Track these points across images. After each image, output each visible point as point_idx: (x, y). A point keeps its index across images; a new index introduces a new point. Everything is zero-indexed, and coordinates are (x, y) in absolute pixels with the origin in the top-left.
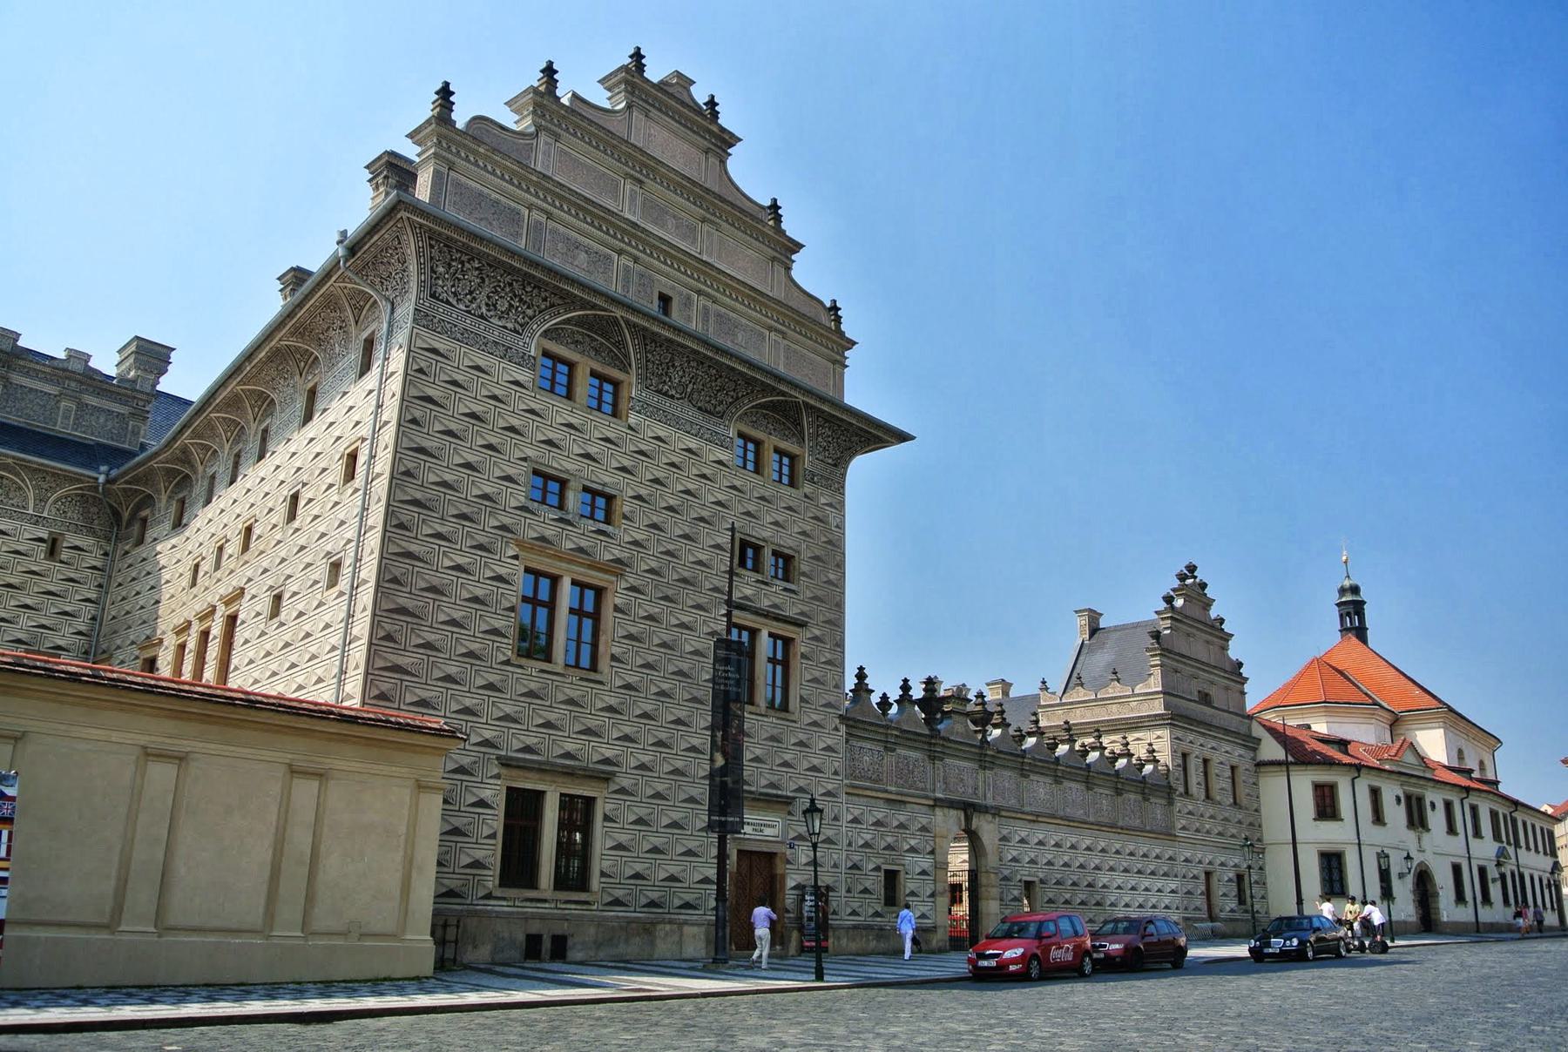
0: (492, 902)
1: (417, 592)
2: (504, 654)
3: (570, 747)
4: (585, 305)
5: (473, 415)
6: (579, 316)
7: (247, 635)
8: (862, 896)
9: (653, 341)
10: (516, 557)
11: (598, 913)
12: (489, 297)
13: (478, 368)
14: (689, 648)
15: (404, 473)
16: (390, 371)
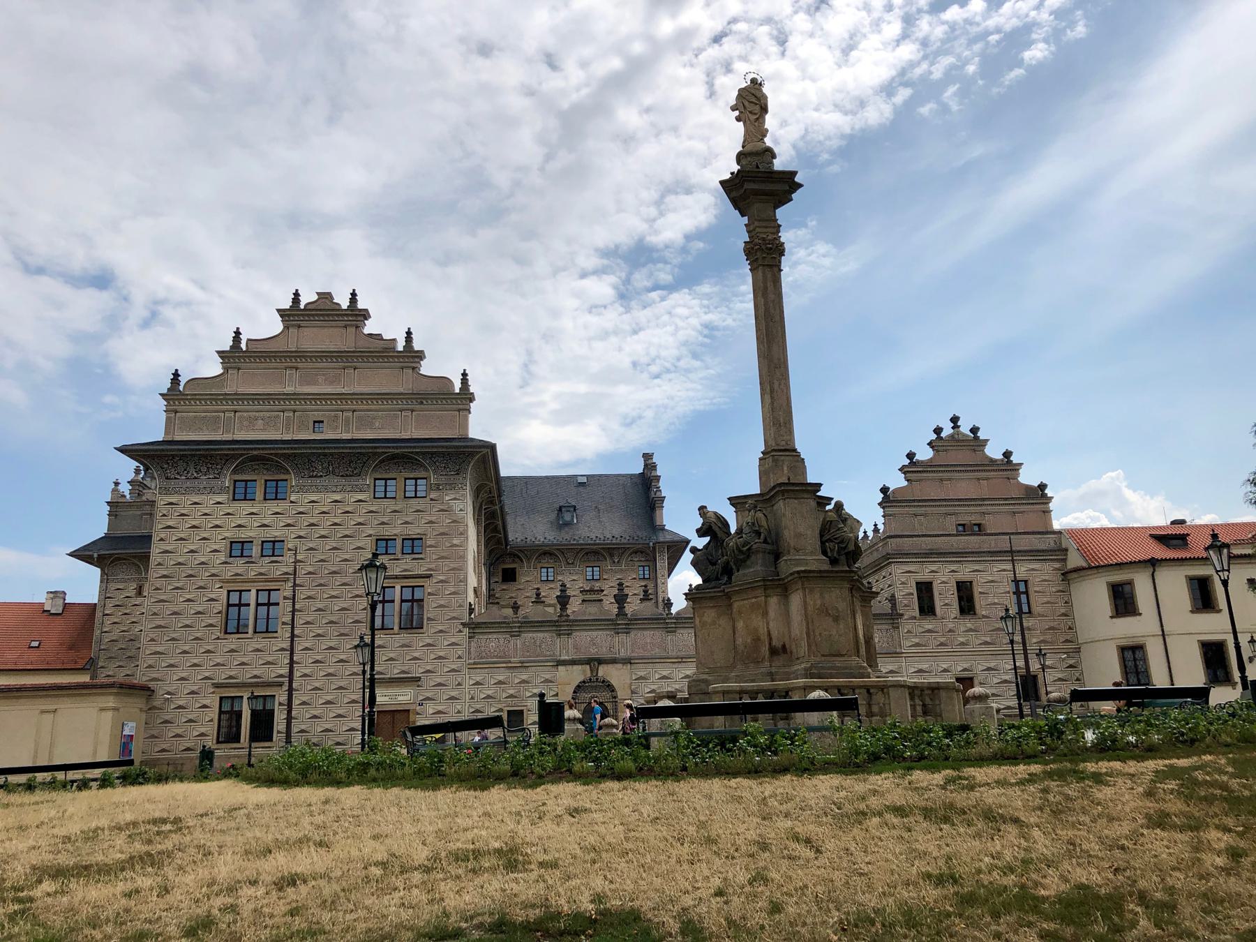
4: (242, 455)
5: (194, 527)
10: (221, 587)
14: (337, 608)
15: (157, 565)
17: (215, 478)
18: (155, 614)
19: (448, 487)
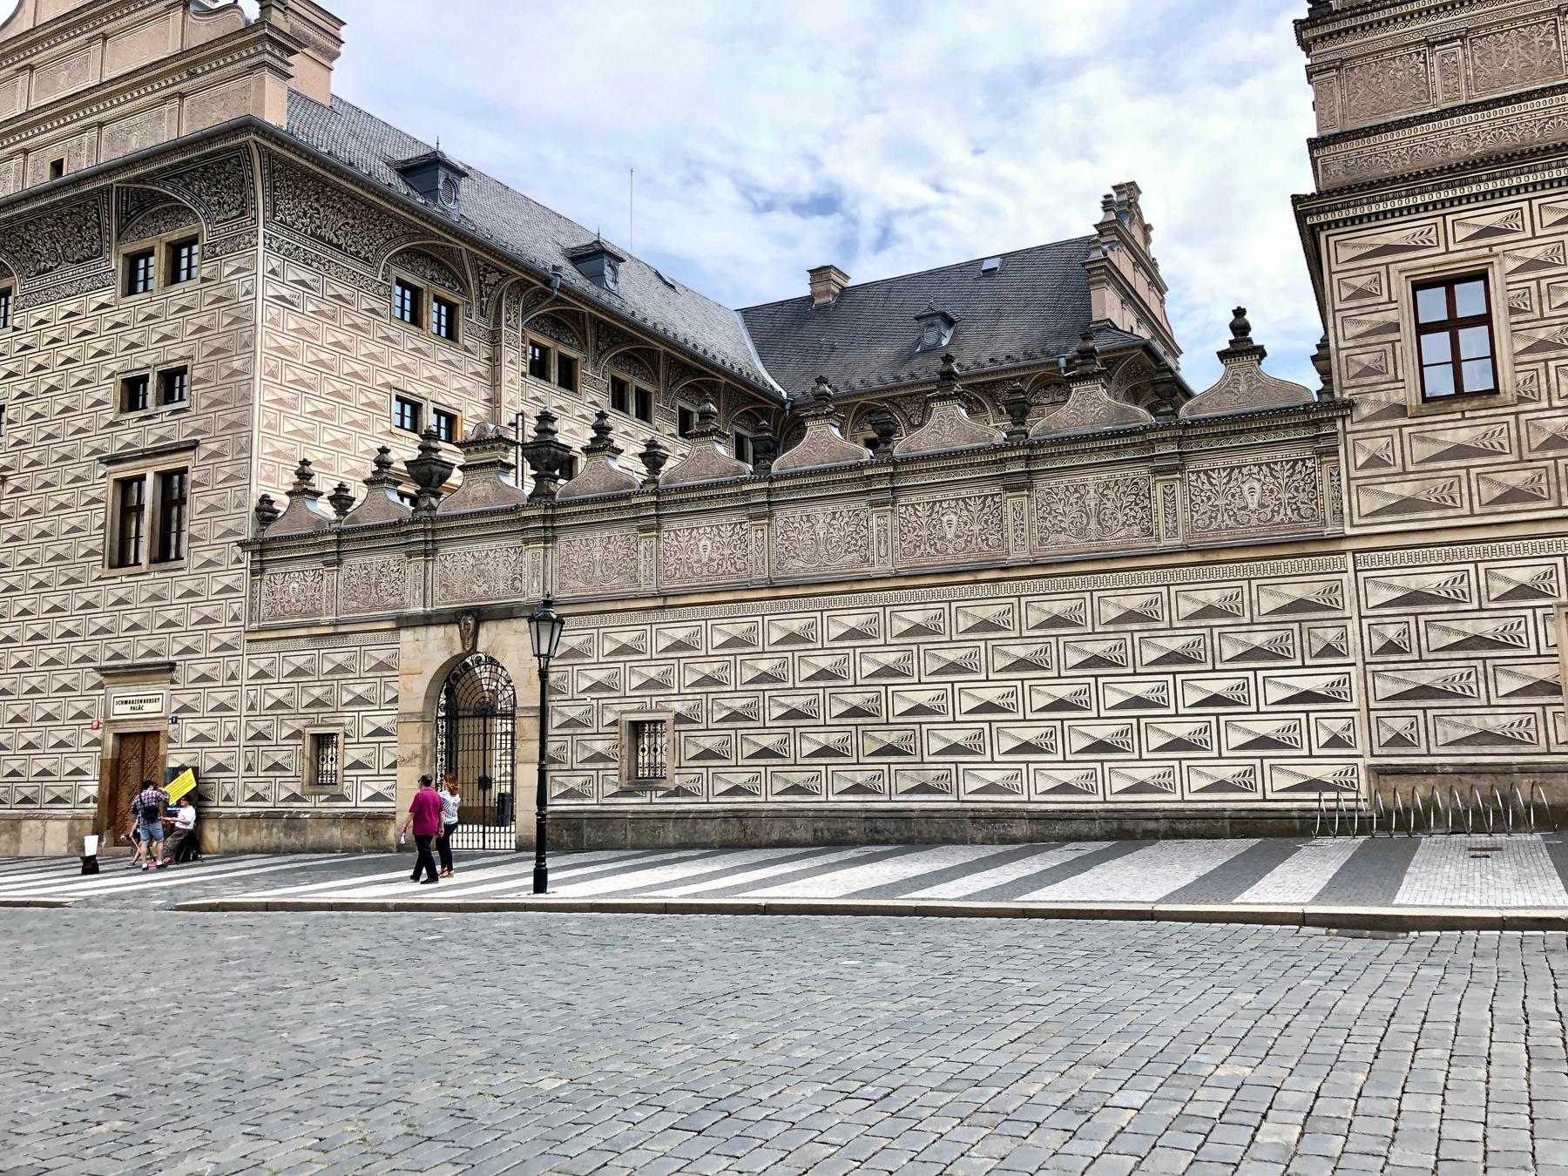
8: (270, 773)
19: (229, 246)
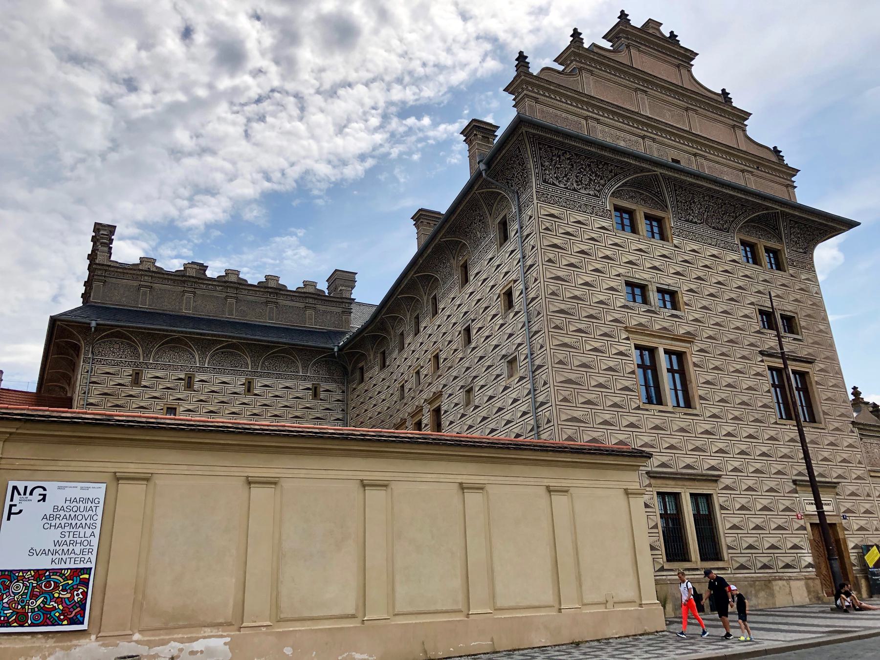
0: (665, 573)
1: (575, 368)
2: (635, 403)
3: (689, 461)
6: (632, 179)
7: (451, 418)
9: (681, 187)
10: (628, 339)
11: (732, 575)
12: (577, 177)
13: (579, 222)
15: (551, 294)
16: (525, 234)
17: (596, 196)
18: (561, 362)
